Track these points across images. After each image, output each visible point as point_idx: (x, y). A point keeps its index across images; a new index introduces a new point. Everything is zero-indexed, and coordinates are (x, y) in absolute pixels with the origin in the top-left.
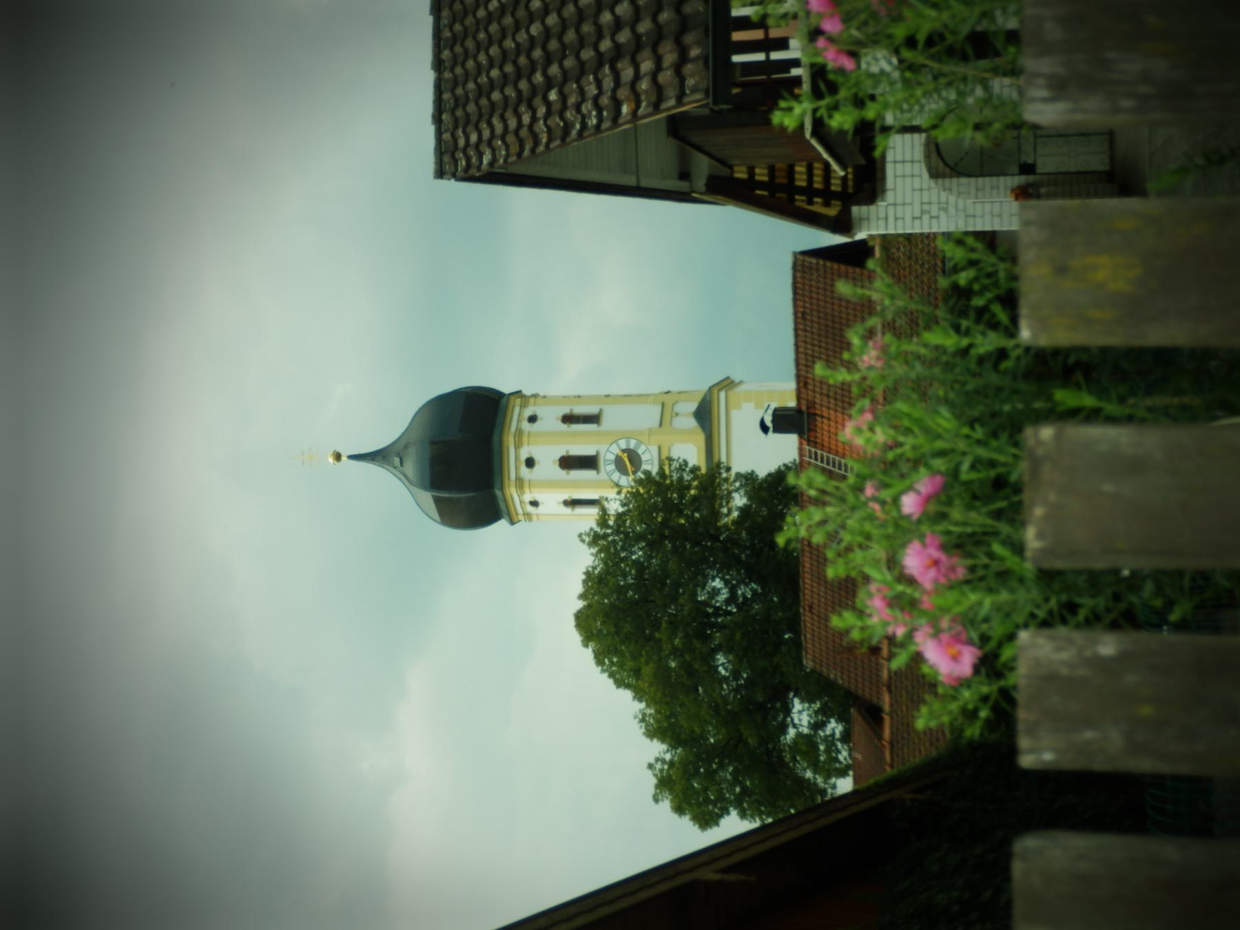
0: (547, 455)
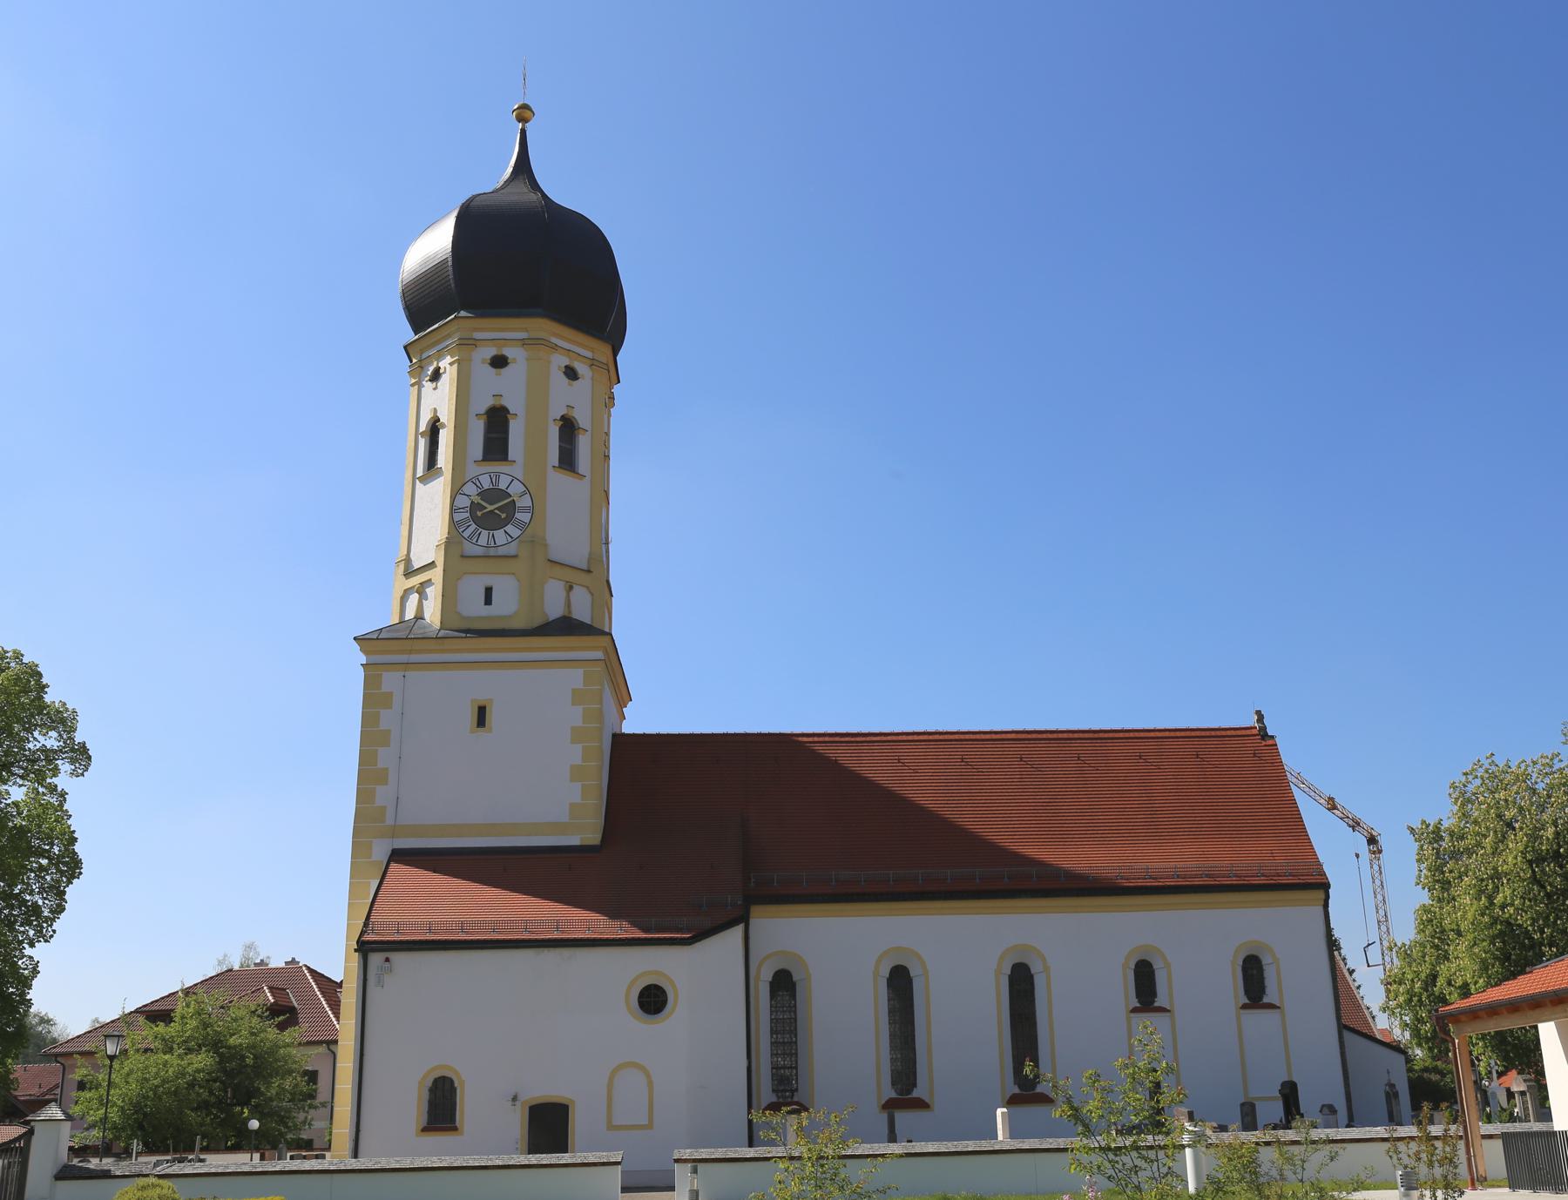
0: (511, 388)
